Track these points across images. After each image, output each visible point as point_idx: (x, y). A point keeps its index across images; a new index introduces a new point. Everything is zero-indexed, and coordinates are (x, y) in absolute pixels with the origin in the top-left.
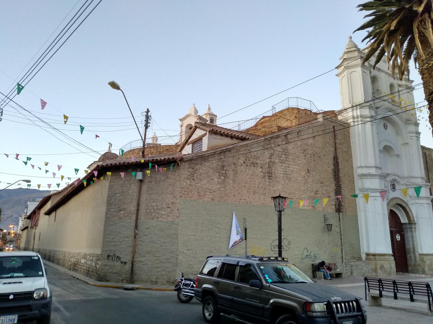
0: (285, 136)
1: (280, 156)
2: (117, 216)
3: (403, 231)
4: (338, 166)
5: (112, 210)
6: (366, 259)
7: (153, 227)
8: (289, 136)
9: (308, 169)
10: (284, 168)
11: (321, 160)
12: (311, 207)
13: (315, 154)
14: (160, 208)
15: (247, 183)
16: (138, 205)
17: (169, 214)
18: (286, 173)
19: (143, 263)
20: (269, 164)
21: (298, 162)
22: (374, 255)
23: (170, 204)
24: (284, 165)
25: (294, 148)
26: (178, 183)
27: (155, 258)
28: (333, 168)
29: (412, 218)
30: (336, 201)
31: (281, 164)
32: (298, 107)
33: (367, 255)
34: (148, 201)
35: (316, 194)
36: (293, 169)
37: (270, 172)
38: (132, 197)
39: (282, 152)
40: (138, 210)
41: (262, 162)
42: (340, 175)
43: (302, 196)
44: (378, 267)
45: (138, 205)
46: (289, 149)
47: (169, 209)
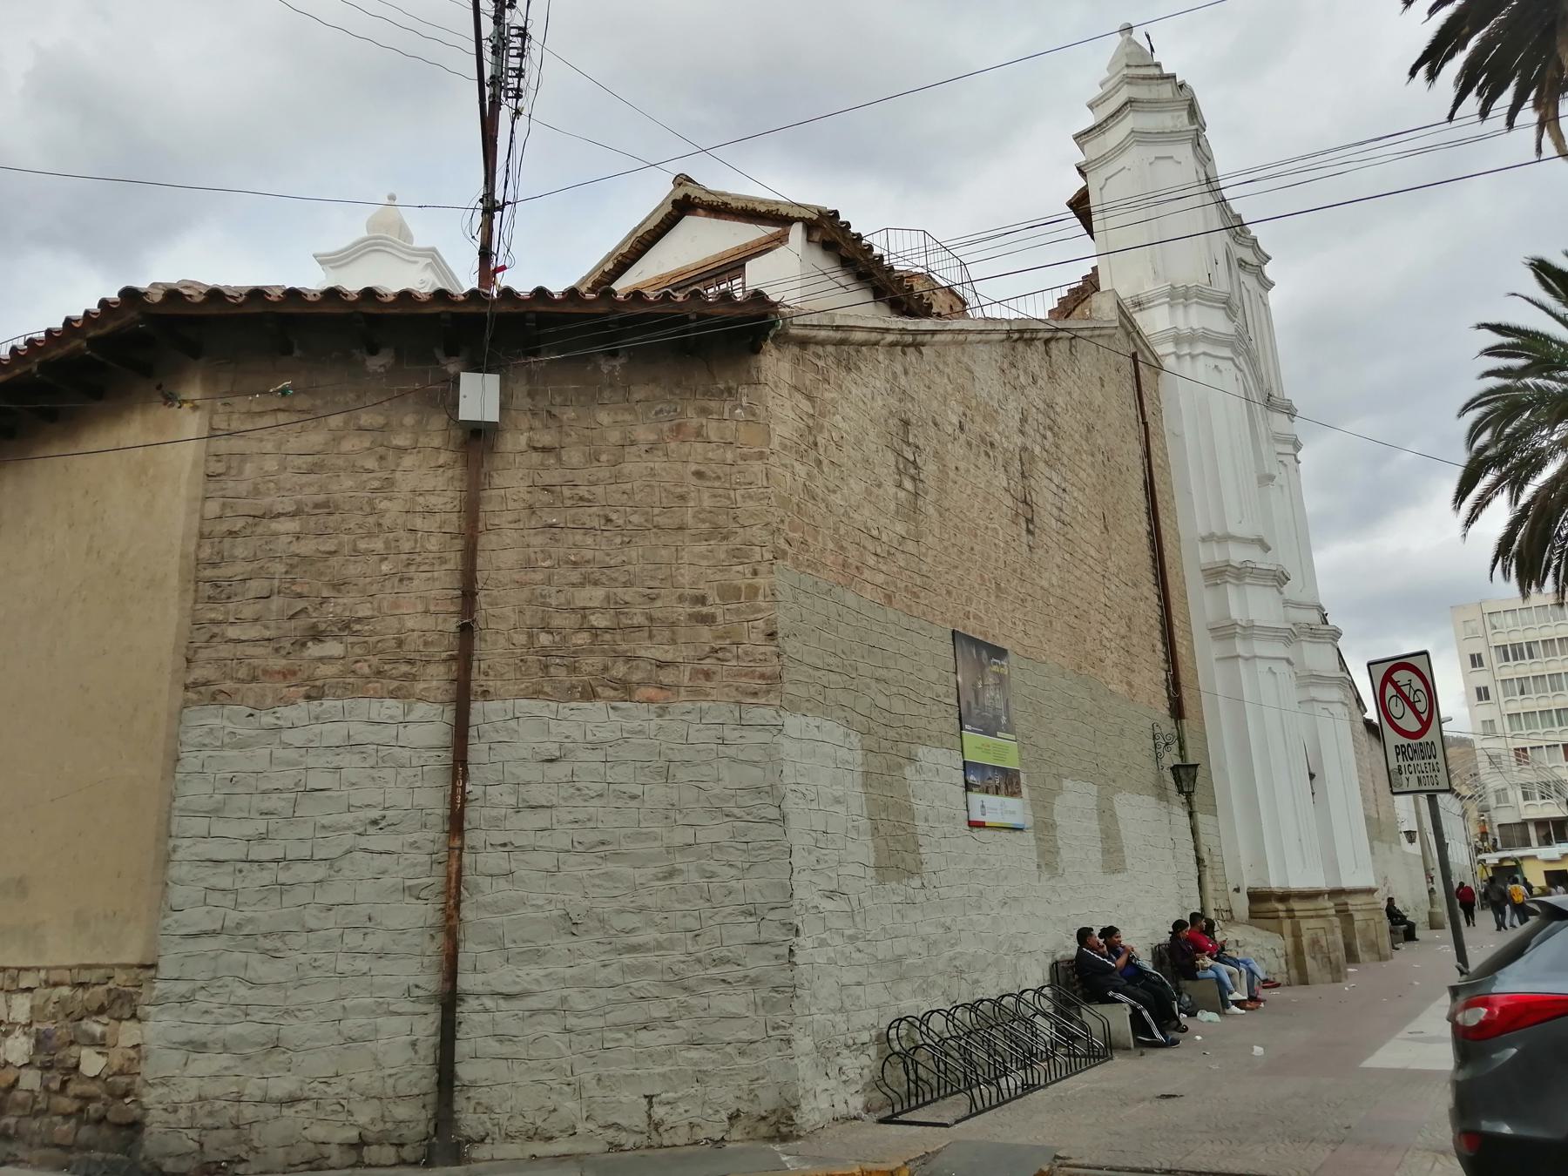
2: (286, 674)
5: (232, 632)
6: (1254, 915)
7: (594, 747)
14: (639, 620)
16: (468, 595)
17: (708, 664)
19: (533, 1003)
22: (1285, 897)
23: (713, 597)
26: (757, 466)
27: (627, 959)
33: (1256, 897)
34: (538, 576)
38: (406, 546)
40: (467, 631)
44: (1305, 941)
45: (468, 595)
47: (705, 632)
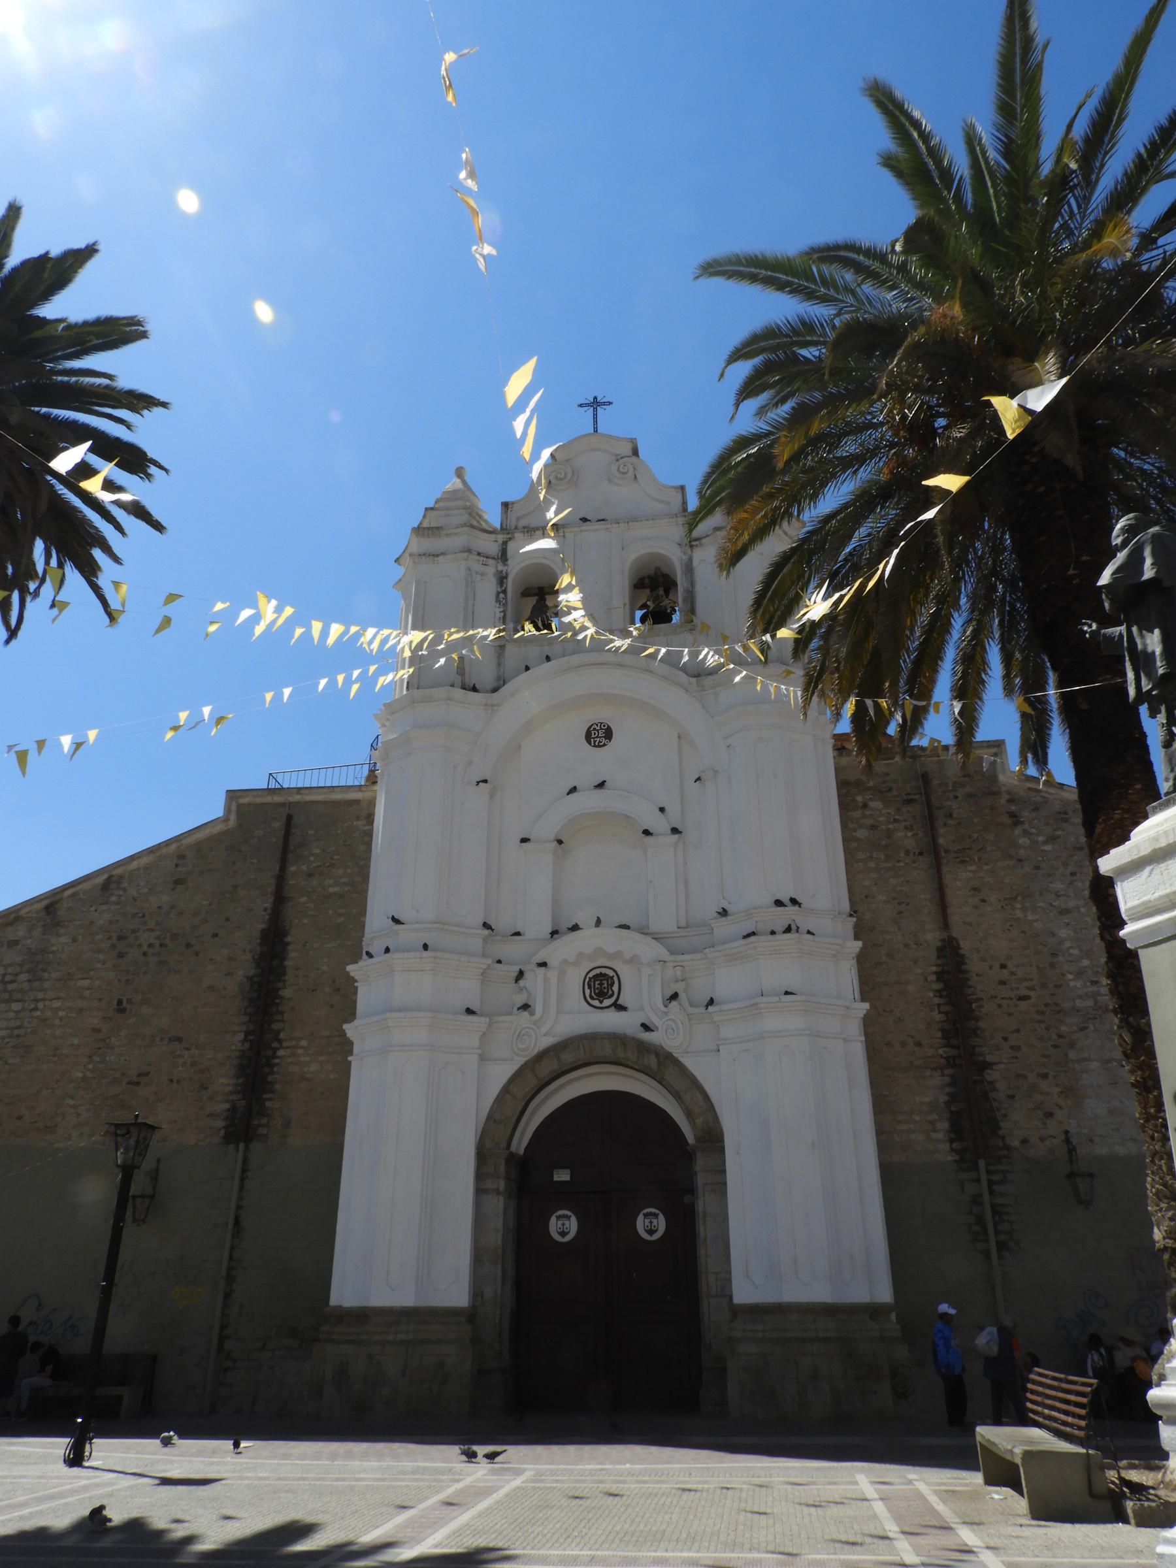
0: (47, 908)
1: (8, 978)
3: (692, 1191)
4: (284, 959)
9: (120, 1002)
10: (12, 1015)
11: (197, 954)
18: (16, 1032)
21: (81, 983)
24: (15, 1006)
25: (75, 940)
28: (252, 972)
30: (235, 1097)
35: (137, 1084)
36: (49, 1013)
39: (21, 965)
42: (286, 993)
43: (72, 1102)
46: (54, 948)
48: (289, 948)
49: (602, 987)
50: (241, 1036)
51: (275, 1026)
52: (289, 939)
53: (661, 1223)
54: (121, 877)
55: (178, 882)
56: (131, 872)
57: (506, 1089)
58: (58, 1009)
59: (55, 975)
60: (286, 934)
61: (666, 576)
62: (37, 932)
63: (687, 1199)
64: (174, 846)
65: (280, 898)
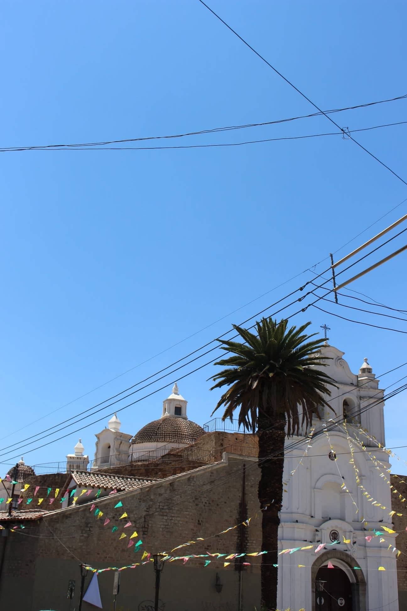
0: (170, 484)
1: (161, 507)
8: (176, 483)
9: (199, 521)
10: (164, 520)
12: (198, 565)
13: (211, 502)
15: (115, 540)
20: (145, 517)
21: (185, 512)
24: (165, 518)
28: (238, 517)
29: (360, 577)
31: (161, 517)
32: (226, 431)
35: (208, 549)
36: (176, 522)
37: (146, 526)
41: (136, 516)
48: (248, 511)
49: (334, 536)
50: (236, 537)
51: (246, 536)
52: (247, 507)
53: (343, 602)
54: (194, 477)
55: (212, 482)
56: (196, 477)
57: (314, 564)
58: (179, 521)
59: (176, 508)
60: (246, 506)
61: (346, 402)
62: (168, 492)
63: (350, 596)
64: (210, 469)
65: (244, 494)
